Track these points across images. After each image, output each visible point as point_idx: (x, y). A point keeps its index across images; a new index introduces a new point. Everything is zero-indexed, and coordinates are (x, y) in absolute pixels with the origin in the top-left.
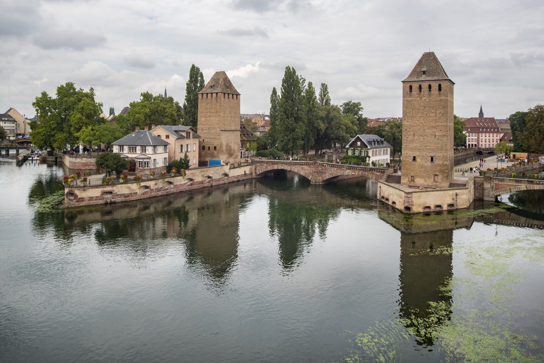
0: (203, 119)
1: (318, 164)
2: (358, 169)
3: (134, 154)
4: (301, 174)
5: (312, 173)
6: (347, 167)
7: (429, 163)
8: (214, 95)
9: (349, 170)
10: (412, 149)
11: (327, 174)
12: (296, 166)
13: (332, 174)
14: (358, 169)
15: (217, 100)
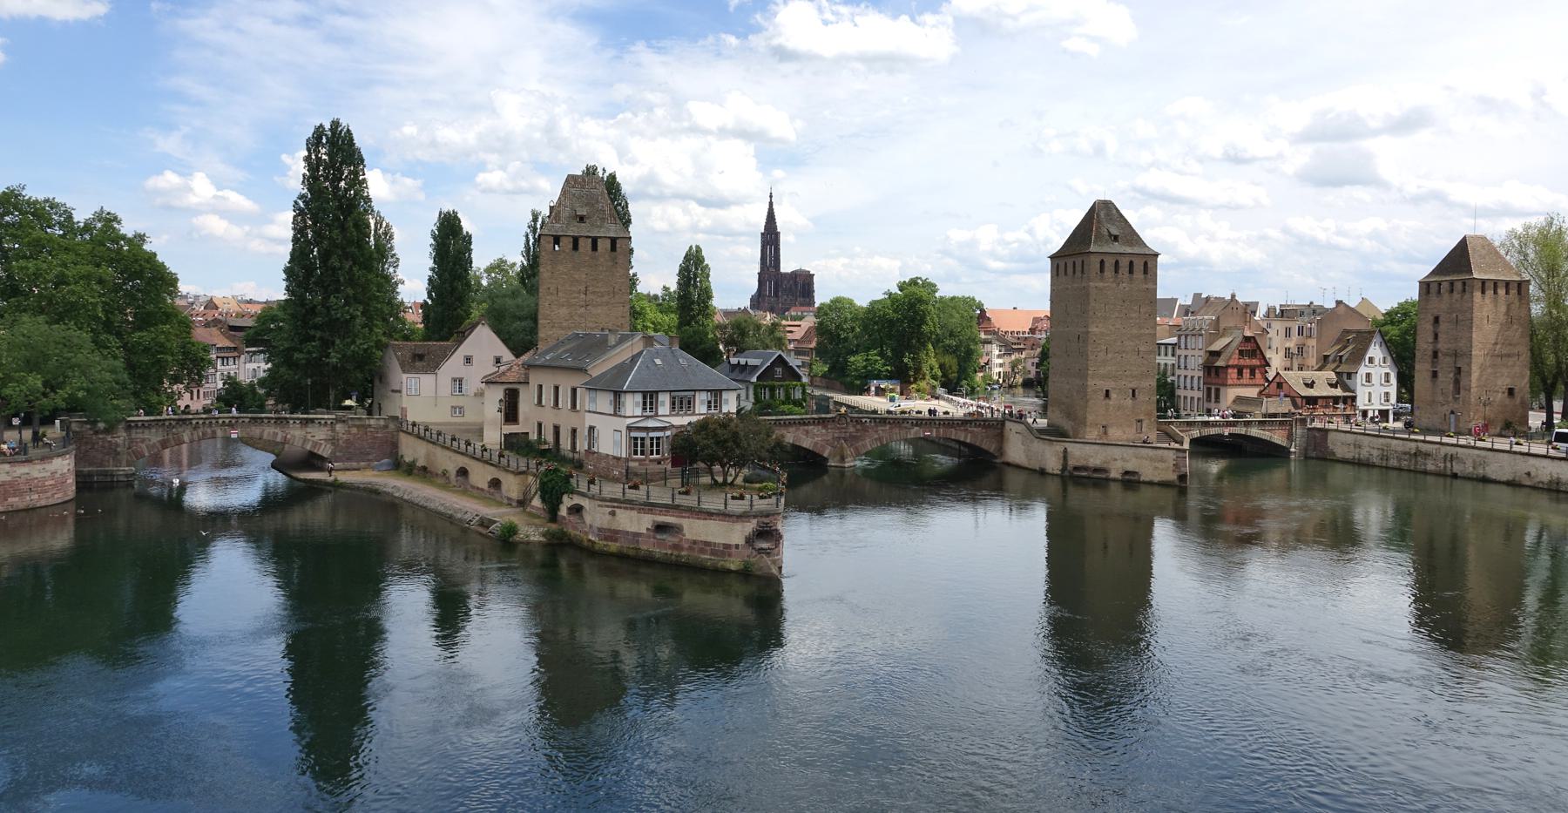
0: (564, 311)
1: (849, 420)
2: (937, 423)
3: (686, 414)
4: (804, 446)
5: (831, 441)
6: (915, 422)
7: (1129, 402)
8: (604, 245)
9: (916, 428)
10: (1103, 377)
11: (867, 441)
12: (791, 429)
13: (880, 439)
14: (937, 423)
15: (614, 261)
